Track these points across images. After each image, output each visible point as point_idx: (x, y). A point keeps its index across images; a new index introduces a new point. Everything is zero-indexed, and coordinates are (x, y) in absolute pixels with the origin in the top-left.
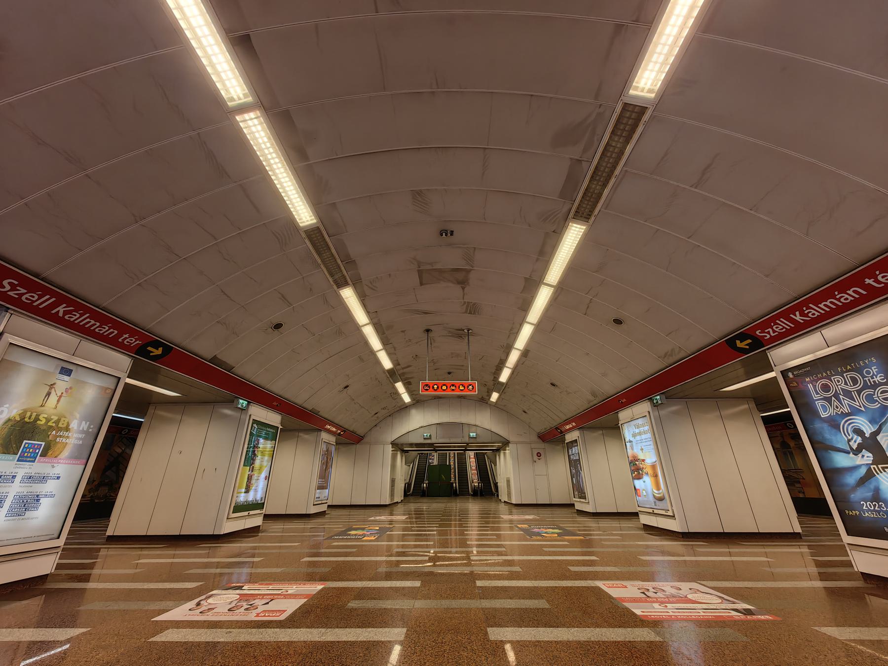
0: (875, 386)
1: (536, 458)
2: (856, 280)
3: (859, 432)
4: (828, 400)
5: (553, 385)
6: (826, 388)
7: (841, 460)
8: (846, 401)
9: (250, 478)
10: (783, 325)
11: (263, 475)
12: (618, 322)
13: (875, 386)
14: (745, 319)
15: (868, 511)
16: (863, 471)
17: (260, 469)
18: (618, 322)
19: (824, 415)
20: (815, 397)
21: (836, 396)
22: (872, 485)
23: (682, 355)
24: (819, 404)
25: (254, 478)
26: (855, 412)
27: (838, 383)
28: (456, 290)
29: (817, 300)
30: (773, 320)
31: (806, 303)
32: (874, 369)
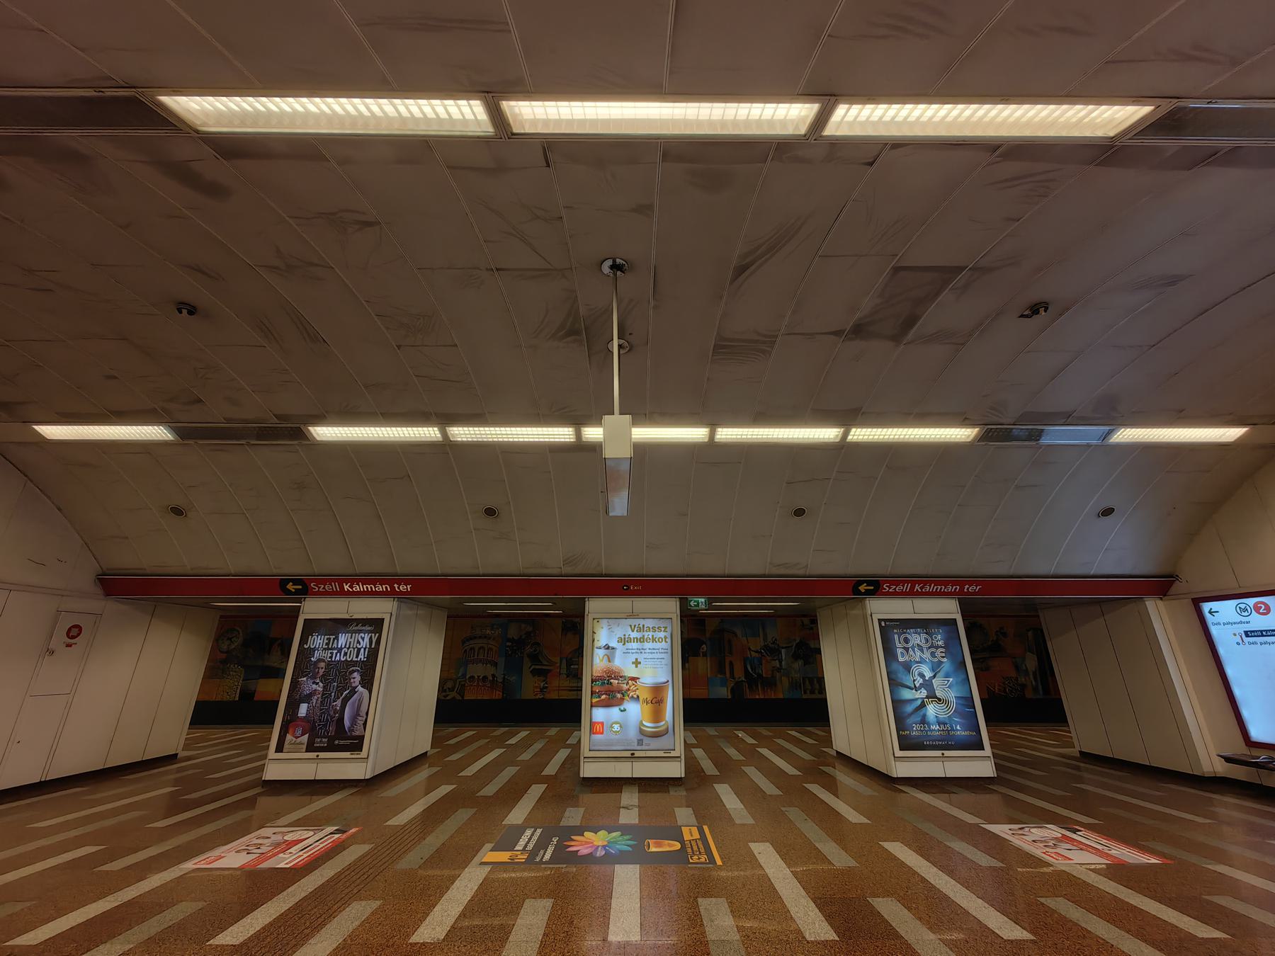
0: (937, 647)
1: (60, 637)
2: (962, 584)
3: (922, 675)
4: (907, 649)
6: (907, 641)
7: (907, 694)
8: (918, 653)
10: (907, 587)
12: (799, 512)
13: (937, 647)
14: (888, 571)
15: (915, 730)
16: (919, 702)
18: (799, 512)
19: (901, 659)
20: (898, 645)
21: (913, 648)
22: (921, 713)
23: (801, 572)
24: (899, 651)
26: (922, 661)
27: (917, 638)
29: (937, 583)
30: (903, 582)
31: (930, 583)
32: (939, 637)
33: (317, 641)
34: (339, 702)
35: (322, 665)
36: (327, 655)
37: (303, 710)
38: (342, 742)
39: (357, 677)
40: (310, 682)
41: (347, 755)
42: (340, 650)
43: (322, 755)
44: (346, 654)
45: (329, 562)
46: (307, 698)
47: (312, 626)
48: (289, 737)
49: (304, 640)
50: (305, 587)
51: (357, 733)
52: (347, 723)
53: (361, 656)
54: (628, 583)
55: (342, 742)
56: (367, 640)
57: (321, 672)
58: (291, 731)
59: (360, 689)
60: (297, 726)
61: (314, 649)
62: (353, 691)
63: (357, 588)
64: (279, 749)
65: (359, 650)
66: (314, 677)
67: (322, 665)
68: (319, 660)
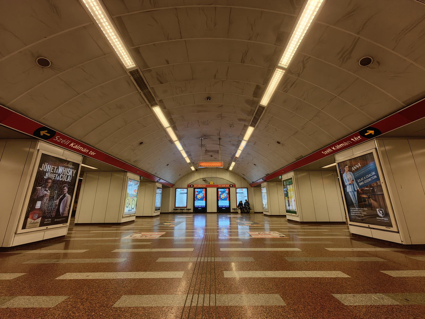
5: (141, 143)
9: (288, 201)
11: (293, 200)
17: (291, 197)
25: (290, 201)
28: (207, 149)
33: (47, 167)
34: (58, 201)
35: (50, 181)
36: (53, 176)
37: (38, 205)
38: (58, 220)
39: (66, 189)
40: (43, 190)
41: (61, 225)
42: (59, 175)
43: (49, 227)
44: (62, 177)
45: (76, 132)
46: (41, 198)
47: (45, 158)
48: (29, 220)
49: (40, 166)
50: (51, 136)
51: (65, 215)
52: (61, 210)
53: (69, 180)
54: (138, 170)
55: (58, 220)
56: (71, 172)
57: (49, 184)
58: (30, 216)
59: (67, 195)
60: (35, 213)
61: (46, 172)
62: (64, 196)
63: (76, 147)
64: (24, 227)
65: (68, 176)
66: (45, 187)
67: (50, 181)
68: (49, 178)
